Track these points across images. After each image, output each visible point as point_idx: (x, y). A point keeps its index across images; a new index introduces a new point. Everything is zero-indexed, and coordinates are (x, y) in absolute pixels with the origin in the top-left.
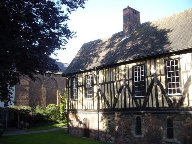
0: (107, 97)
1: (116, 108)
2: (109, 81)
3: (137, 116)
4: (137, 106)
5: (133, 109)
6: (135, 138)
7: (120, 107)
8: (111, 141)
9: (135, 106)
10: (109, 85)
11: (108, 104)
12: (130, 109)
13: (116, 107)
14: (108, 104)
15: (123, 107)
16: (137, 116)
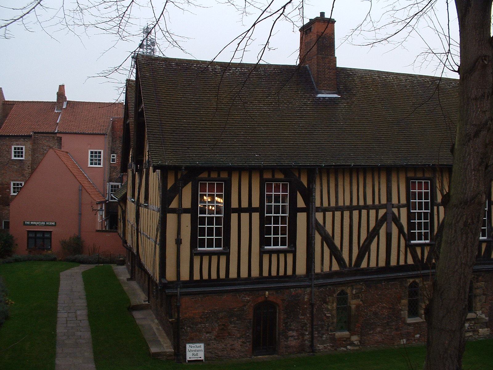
0: (337, 242)
1: (363, 269)
2: (347, 203)
3: (411, 280)
4: (414, 260)
5: (406, 268)
6: (409, 325)
7: (373, 264)
8: (352, 344)
9: (410, 261)
10: (347, 214)
11: (340, 260)
12: (399, 268)
13: (364, 265)
14: (340, 260)
15: (382, 264)
16: (411, 280)
